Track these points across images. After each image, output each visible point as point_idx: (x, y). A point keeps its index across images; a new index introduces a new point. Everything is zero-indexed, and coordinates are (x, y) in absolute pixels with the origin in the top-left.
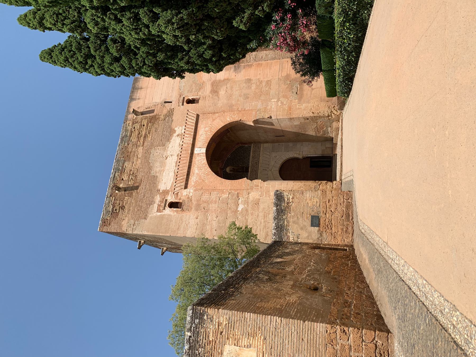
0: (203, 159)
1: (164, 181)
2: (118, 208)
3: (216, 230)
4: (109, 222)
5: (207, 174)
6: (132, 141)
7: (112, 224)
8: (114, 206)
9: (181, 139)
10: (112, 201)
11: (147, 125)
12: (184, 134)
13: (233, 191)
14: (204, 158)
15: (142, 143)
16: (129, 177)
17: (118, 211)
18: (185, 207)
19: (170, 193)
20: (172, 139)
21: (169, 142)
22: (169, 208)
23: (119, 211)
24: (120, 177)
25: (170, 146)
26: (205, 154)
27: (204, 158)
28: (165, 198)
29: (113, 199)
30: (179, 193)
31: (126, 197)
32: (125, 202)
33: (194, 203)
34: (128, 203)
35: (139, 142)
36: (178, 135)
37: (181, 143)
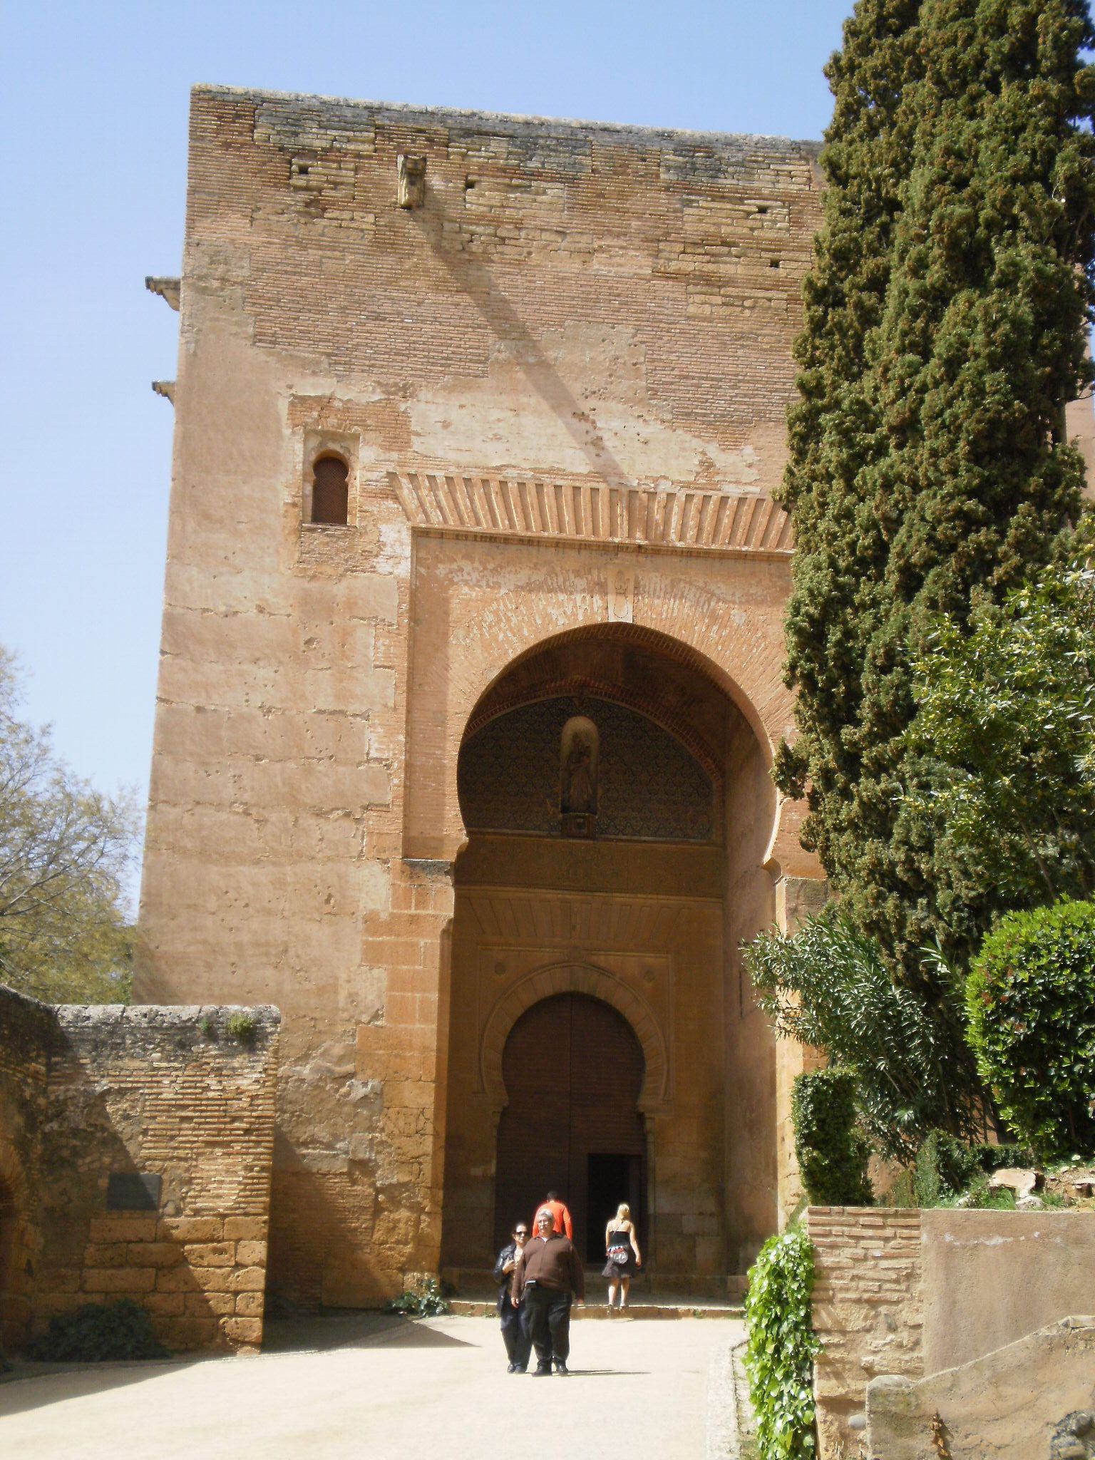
0: (574, 614)
1: (455, 415)
2: (314, 180)
3: (199, 709)
4: (241, 139)
5: (495, 637)
6: (688, 211)
7: (231, 158)
8: (324, 155)
9: (687, 485)
10: (349, 140)
11: (777, 285)
12: (716, 496)
13: (396, 781)
14: (581, 618)
15: (673, 266)
16: (480, 219)
17: (299, 181)
18: (319, 539)
19: (395, 455)
20: (688, 437)
21: (668, 416)
22: (313, 457)
23: (297, 189)
24: (481, 167)
25: (653, 429)
26: (599, 620)
27: (581, 618)
28: (366, 428)
29: (361, 147)
30: (390, 504)
31: (371, 218)
32: (347, 215)
33: (340, 590)
34: (342, 234)
35: (679, 247)
36: (708, 465)
37: (665, 487)
